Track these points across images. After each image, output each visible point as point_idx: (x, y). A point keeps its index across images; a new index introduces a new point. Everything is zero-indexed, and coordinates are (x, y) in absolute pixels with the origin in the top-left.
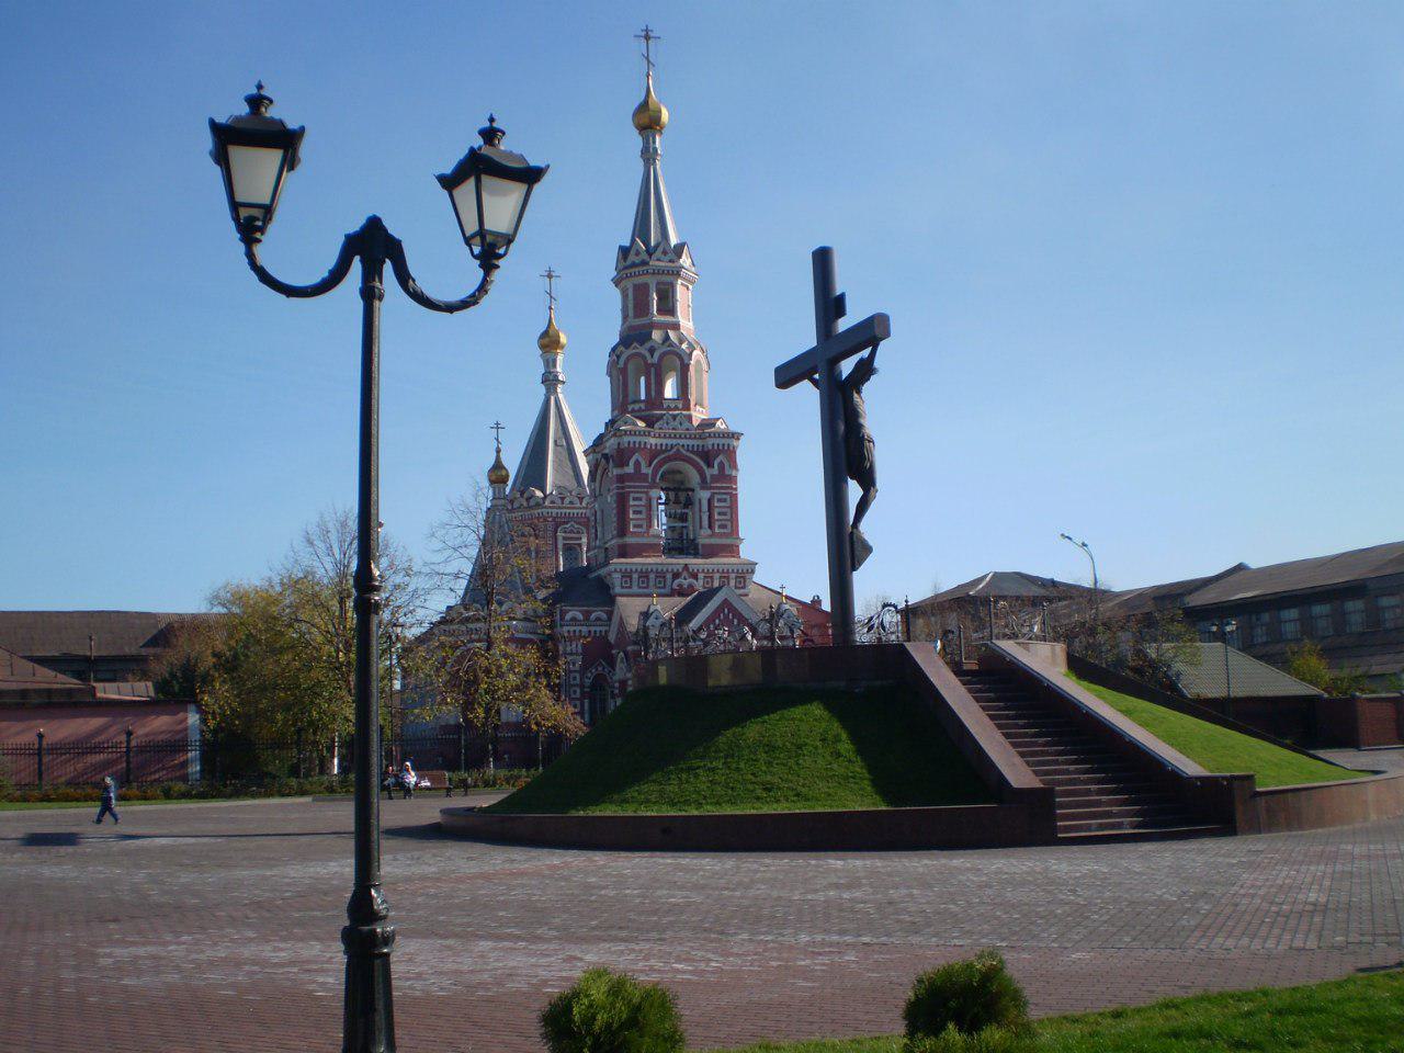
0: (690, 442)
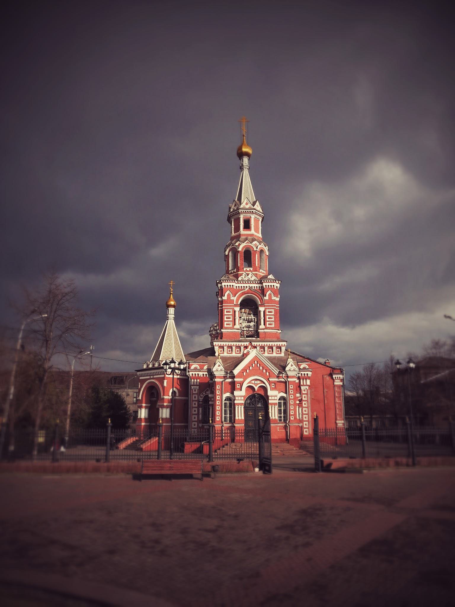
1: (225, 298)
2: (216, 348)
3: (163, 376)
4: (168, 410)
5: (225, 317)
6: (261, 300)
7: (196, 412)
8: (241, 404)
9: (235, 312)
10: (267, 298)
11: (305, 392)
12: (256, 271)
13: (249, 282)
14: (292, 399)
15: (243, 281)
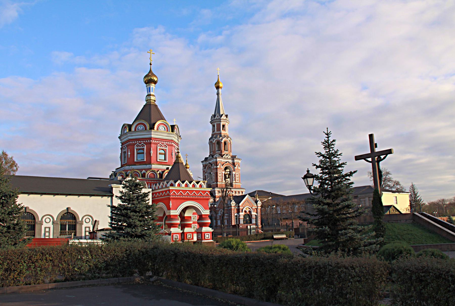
1: (218, 167)
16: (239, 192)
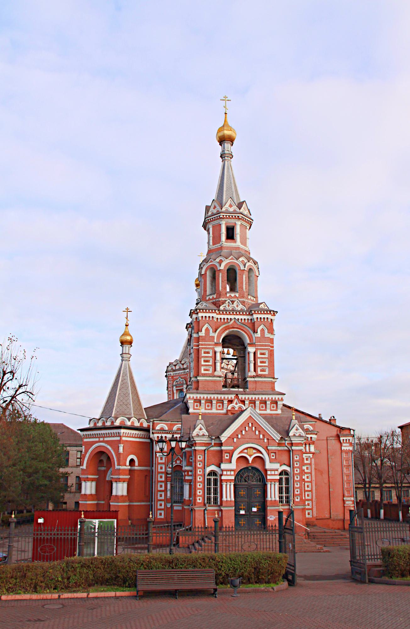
0: (243, 317)
1: (202, 334)
2: (190, 403)
3: (118, 438)
4: (125, 485)
5: (202, 360)
6: (251, 338)
7: (163, 488)
8: (230, 481)
9: (215, 353)
10: (259, 335)
11: (308, 462)
12: (243, 297)
13: (234, 311)
14: (297, 474)
15: (225, 312)
16: (222, 402)
